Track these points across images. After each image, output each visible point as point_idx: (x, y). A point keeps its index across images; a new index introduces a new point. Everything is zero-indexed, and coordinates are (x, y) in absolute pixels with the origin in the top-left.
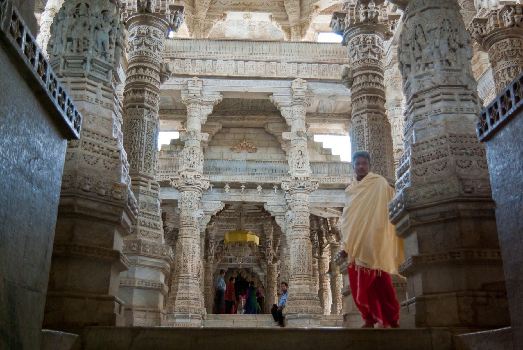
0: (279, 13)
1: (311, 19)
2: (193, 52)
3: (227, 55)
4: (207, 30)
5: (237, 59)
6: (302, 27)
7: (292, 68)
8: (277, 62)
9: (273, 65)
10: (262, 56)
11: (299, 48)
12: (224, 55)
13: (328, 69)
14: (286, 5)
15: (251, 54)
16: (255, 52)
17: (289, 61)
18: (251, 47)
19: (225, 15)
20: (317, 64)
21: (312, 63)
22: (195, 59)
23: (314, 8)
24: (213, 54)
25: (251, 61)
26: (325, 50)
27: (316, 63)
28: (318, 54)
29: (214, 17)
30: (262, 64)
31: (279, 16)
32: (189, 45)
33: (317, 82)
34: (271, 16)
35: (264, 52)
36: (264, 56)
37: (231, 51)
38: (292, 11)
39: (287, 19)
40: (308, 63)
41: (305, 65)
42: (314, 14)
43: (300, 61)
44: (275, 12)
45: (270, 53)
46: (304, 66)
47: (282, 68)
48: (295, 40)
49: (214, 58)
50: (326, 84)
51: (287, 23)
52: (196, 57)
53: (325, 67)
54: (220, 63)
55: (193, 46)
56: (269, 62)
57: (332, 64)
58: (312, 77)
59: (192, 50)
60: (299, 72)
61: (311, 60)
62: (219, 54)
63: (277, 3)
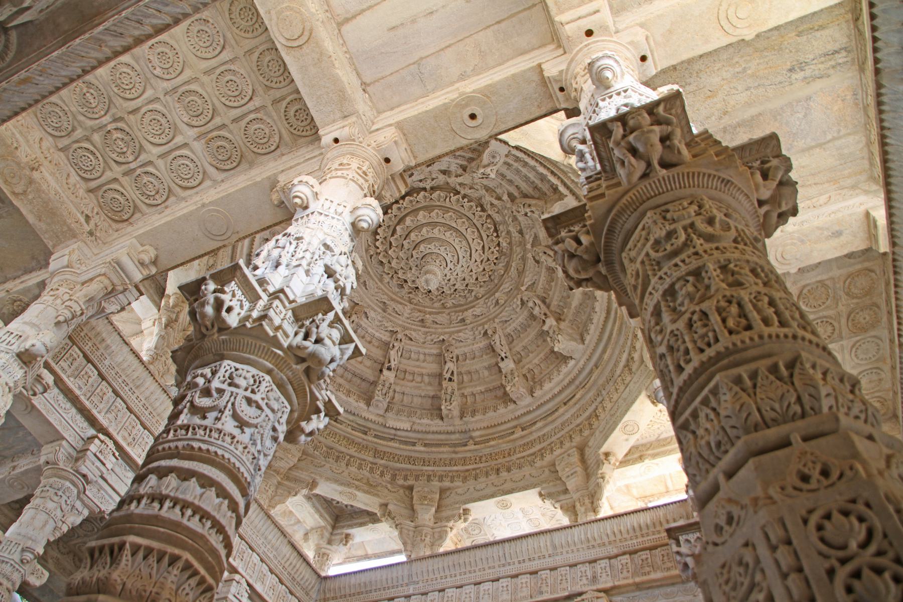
0: (551, 484)
1: (603, 478)
2: (407, 585)
3: (463, 577)
4: (437, 543)
5: (478, 580)
6: (593, 497)
7: (579, 574)
8: (551, 570)
9: (544, 576)
10: (523, 565)
11: (586, 534)
12: (458, 577)
13: (649, 560)
14: (558, 468)
15: (504, 565)
16: (509, 560)
17: (572, 561)
18: (501, 554)
19: (466, 512)
20: (627, 556)
21: (616, 556)
22: (409, 596)
23: (602, 457)
24: (439, 580)
25: (503, 578)
26: (635, 525)
27: (624, 554)
28: (625, 536)
29: (448, 519)
30: (524, 579)
31: (553, 490)
32: (400, 573)
33: (633, 591)
34: (541, 495)
35: (526, 558)
36: (527, 564)
37: (468, 568)
38: (569, 474)
39: (566, 491)
40: (610, 558)
41: (604, 563)
42: (606, 468)
43: (593, 557)
44: (544, 485)
45: (536, 556)
46: (603, 565)
47: (560, 578)
48: (585, 520)
49: (440, 587)
50: (650, 591)
51: (567, 496)
52: (411, 592)
53: (644, 557)
54: (450, 595)
55: (406, 573)
56: (536, 573)
57: (655, 548)
58: (617, 583)
59: (406, 581)
60: (594, 579)
61: (615, 551)
62: (449, 579)
63: (547, 471)
